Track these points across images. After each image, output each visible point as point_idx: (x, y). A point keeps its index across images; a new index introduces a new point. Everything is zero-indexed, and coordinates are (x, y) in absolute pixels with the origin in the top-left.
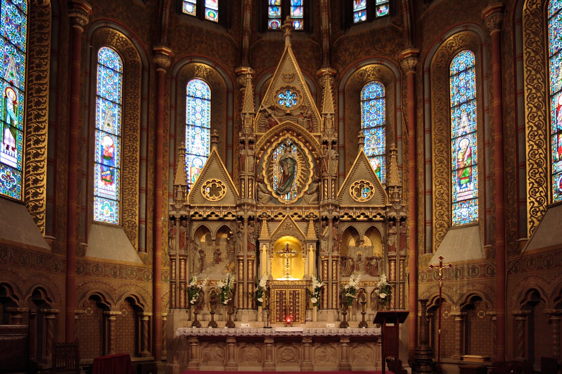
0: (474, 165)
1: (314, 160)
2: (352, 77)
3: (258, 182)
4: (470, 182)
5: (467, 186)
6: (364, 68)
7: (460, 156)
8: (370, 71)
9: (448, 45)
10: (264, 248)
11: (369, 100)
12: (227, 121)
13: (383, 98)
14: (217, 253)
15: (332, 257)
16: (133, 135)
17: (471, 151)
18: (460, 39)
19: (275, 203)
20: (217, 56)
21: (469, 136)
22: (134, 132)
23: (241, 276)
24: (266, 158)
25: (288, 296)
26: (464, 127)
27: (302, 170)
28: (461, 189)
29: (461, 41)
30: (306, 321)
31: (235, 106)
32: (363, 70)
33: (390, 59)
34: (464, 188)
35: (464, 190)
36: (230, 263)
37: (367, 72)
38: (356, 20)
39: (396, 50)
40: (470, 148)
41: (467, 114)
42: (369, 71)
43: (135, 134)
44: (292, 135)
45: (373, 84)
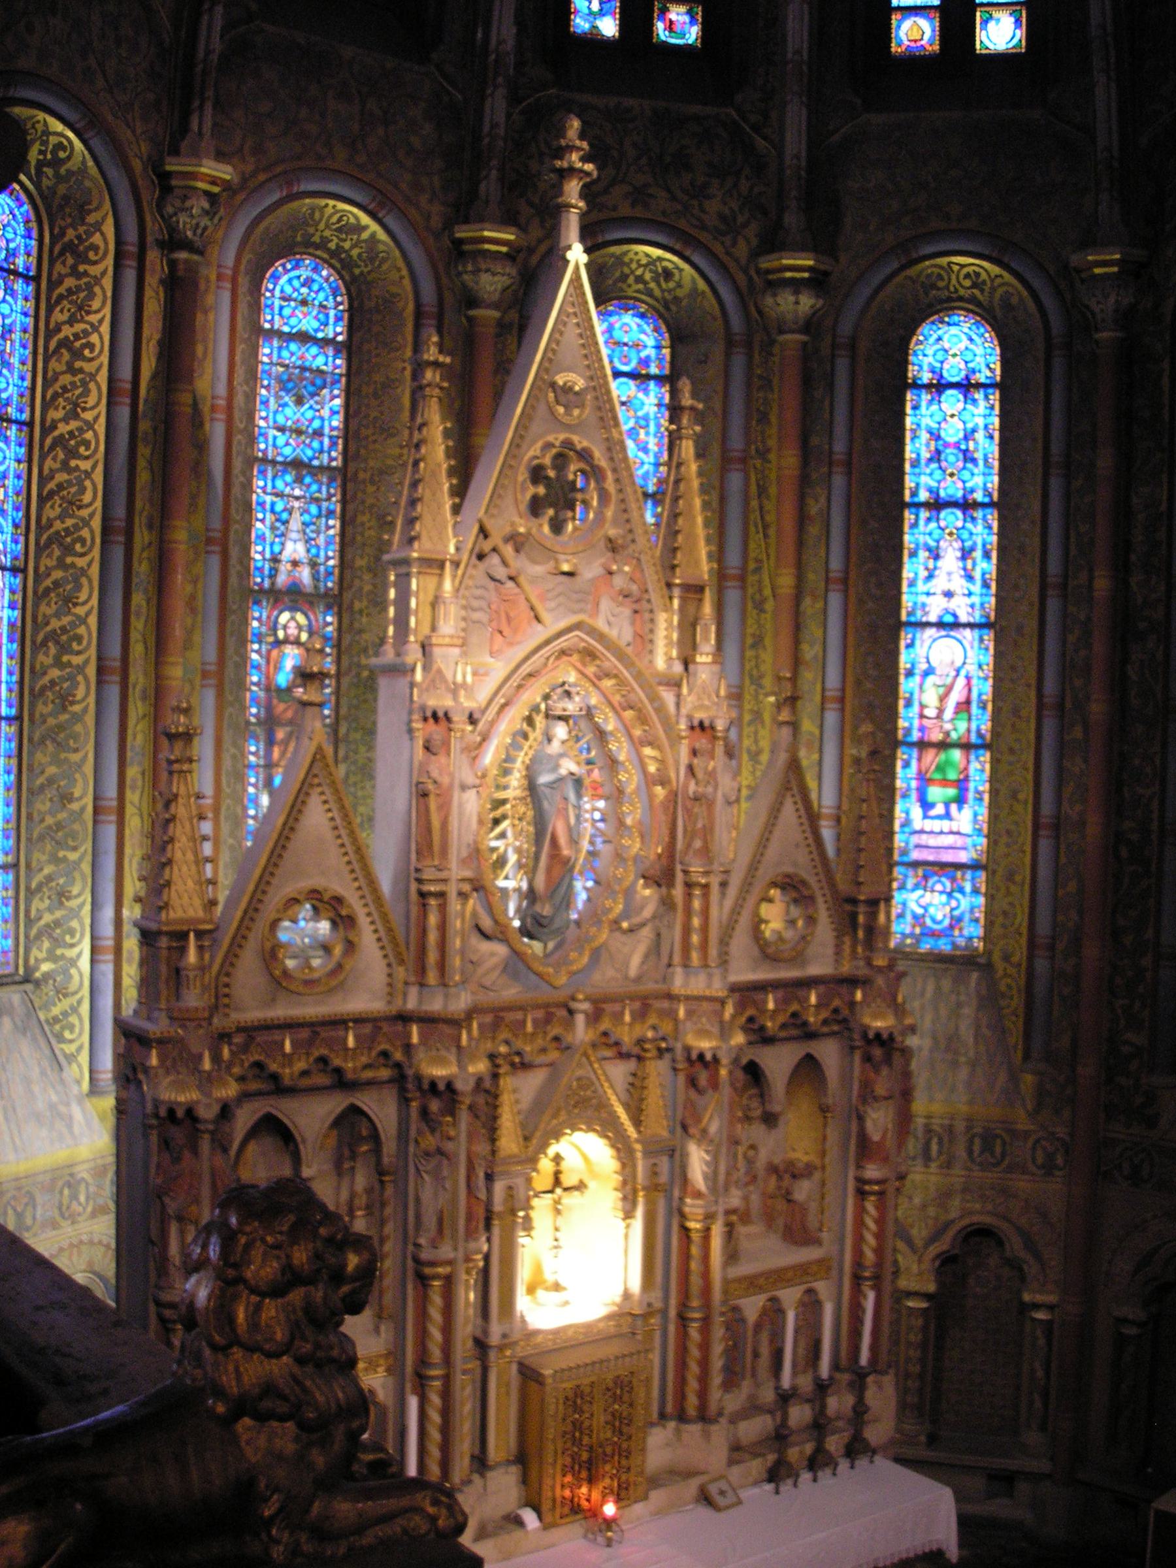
0: (976, 747)
4: (961, 800)
5: (947, 816)
7: (931, 698)
8: (634, 266)
9: (922, 279)
13: (660, 379)
17: (970, 690)
18: (967, 276)
20: (100, 83)
21: (967, 633)
28: (925, 817)
29: (967, 283)
32: (612, 255)
33: (718, 249)
34: (939, 817)
35: (936, 825)
37: (623, 264)
39: (740, 220)
40: (968, 679)
41: (963, 549)
42: (628, 265)
45: (627, 310)
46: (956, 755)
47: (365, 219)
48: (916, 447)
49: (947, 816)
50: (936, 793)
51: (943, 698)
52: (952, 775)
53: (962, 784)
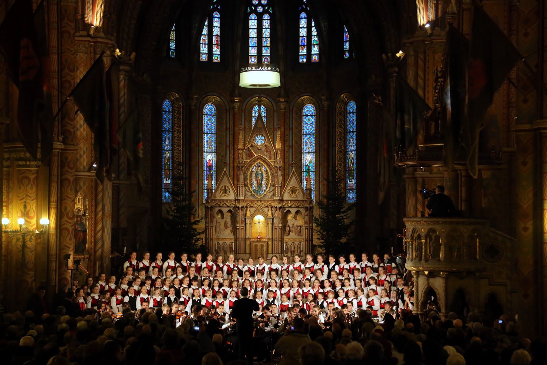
1: (272, 174)
2: (297, 102)
3: (245, 186)
6: (304, 97)
10: (248, 221)
11: (307, 116)
12: (226, 130)
14: (226, 223)
15: (279, 227)
16: (179, 149)
19: (253, 197)
22: (179, 147)
23: (238, 237)
24: (249, 173)
25: (259, 246)
26: (351, 146)
27: (266, 179)
30: (267, 259)
31: (231, 120)
36: (232, 229)
38: (301, 60)
43: (180, 148)
44: (261, 161)
46: (353, 171)
47: (265, 99)
48: (348, 123)
49: (352, 181)
50: (351, 178)
51: (351, 162)
52: (352, 175)
53: (353, 176)
